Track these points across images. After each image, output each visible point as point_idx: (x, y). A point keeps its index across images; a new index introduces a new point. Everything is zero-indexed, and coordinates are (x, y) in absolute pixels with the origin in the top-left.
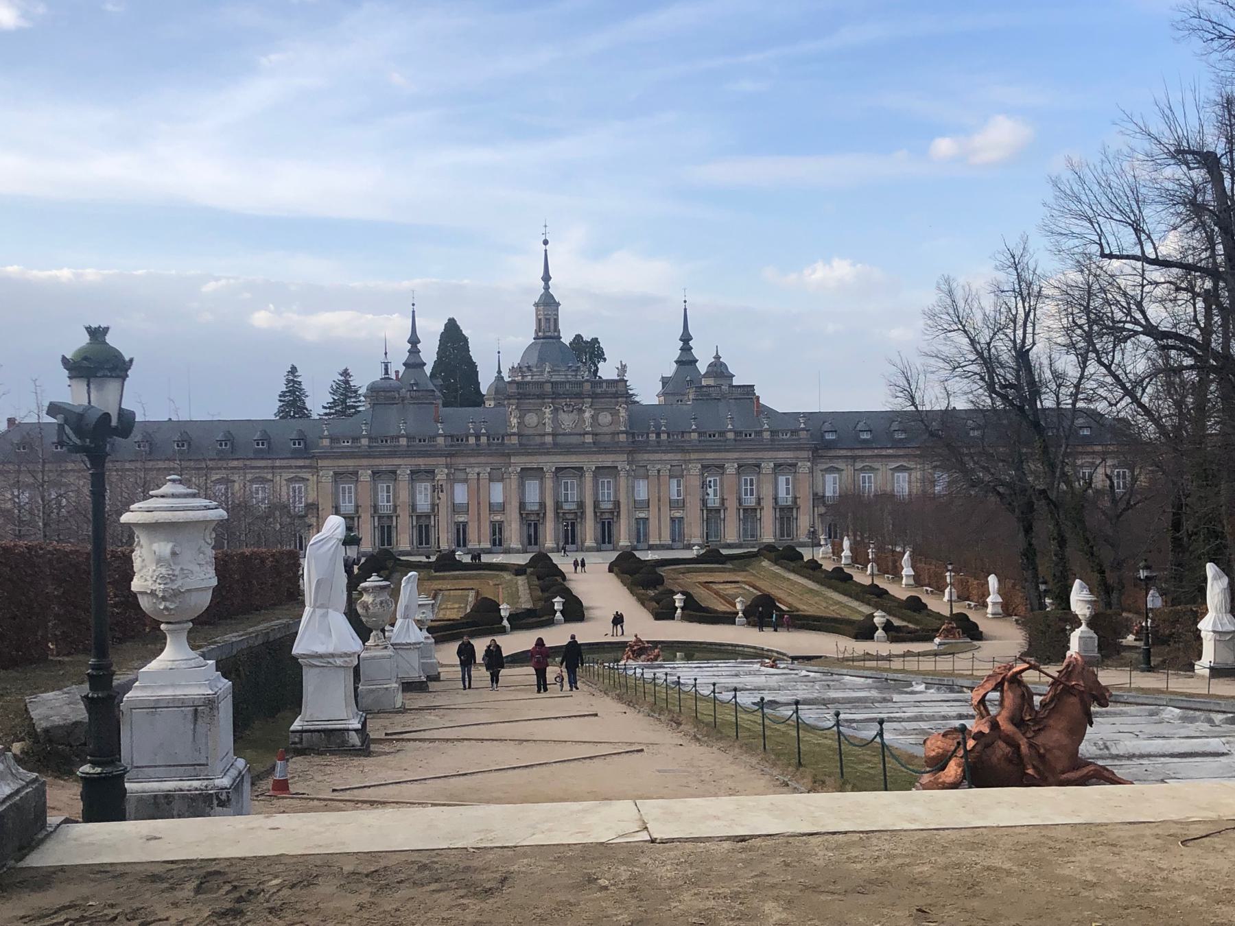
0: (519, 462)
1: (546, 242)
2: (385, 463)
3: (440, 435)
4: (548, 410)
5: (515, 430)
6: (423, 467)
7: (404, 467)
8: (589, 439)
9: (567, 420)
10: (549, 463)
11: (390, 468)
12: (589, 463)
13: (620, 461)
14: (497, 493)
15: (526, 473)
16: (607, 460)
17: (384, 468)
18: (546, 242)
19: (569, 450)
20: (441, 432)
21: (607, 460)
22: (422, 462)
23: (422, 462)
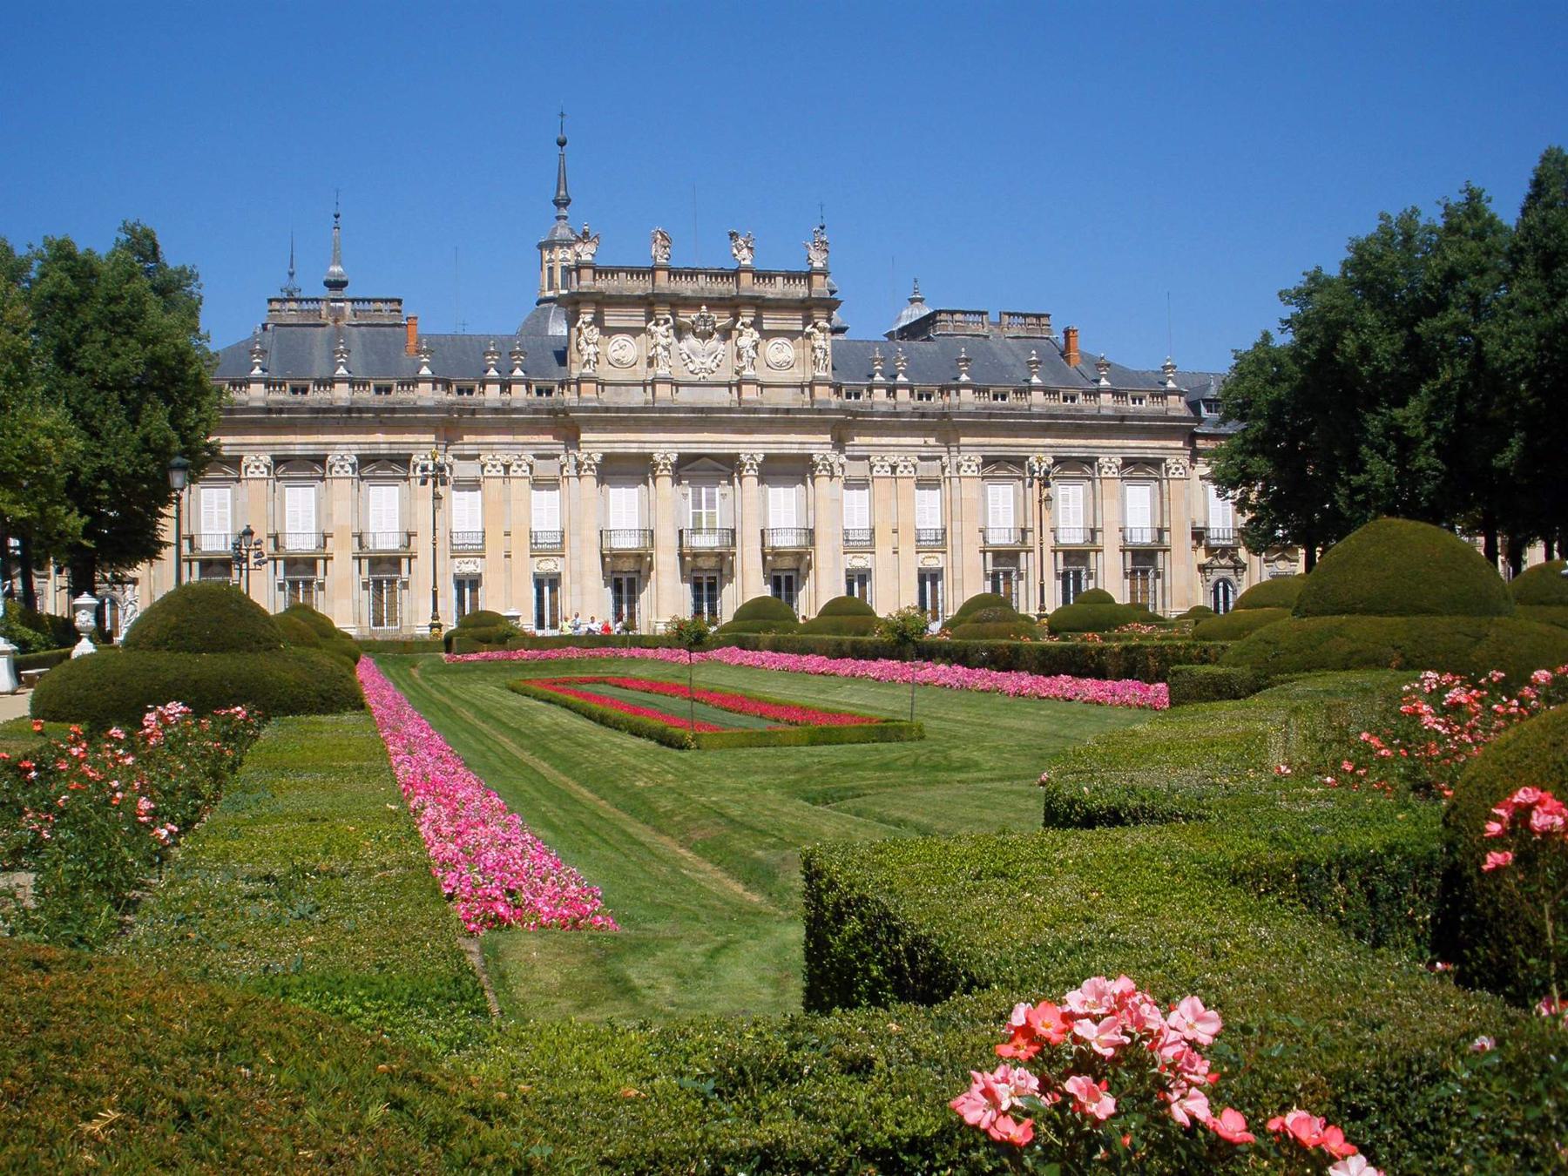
0: (596, 444)
1: (562, 144)
2: (299, 443)
3: (425, 380)
4: (662, 329)
5: (587, 370)
6: (384, 450)
7: (344, 447)
8: (750, 393)
9: (702, 357)
10: (665, 446)
11: (311, 450)
12: (753, 447)
13: (818, 445)
14: (545, 512)
15: (617, 470)
16: (790, 443)
17: (297, 451)
18: (562, 144)
19: (704, 419)
20: (425, 371)
21: (790, 443)
22: (381, 441)
23: (381, 441)
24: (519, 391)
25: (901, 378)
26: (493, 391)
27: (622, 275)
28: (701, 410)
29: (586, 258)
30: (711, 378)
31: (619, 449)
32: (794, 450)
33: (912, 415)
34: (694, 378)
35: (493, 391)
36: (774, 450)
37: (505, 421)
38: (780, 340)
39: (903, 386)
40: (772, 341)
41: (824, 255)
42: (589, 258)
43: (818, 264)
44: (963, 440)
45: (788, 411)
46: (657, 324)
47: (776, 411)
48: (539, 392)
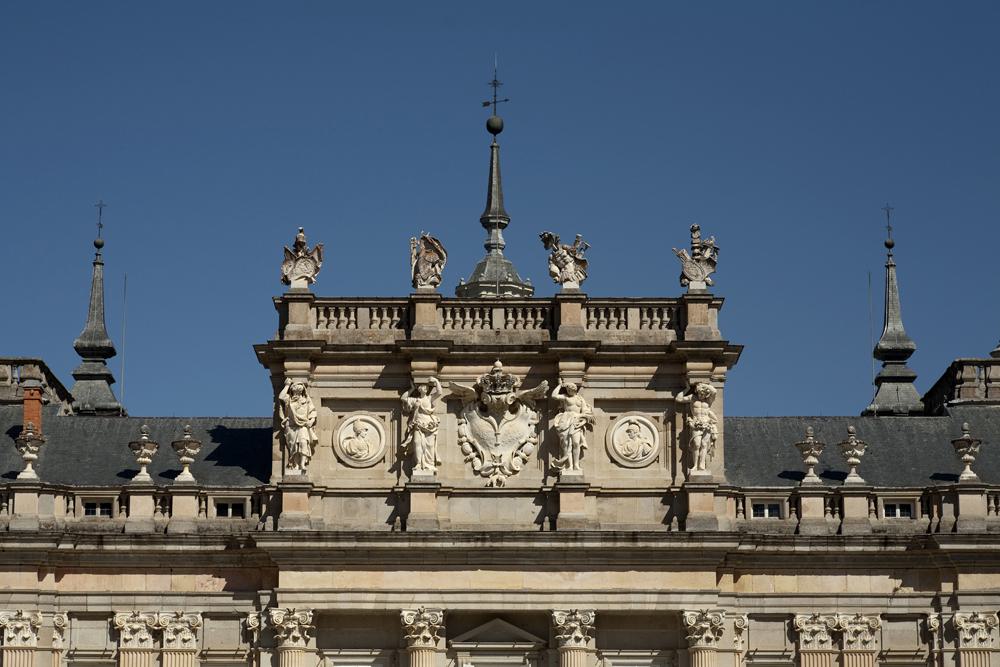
4: (425, 402)
5: (293, 472)
16: (642, 589)
21: (642, 589)
24: (186, 508)
25: (854, 478)
26: (142, 509)
27: (363, 312)
28: (482, 536)
29: (299, 284)
30: (509, 482)
31: (344, 603)
32: (651, 604)
33: (866, 540)
34: (479, 482)
35: (142, 509)
36: (614, 604)
37: (155, 554)
38: (634, 416)
39: (855, 492)
40: (622, 418)
41: (707, 270)
42: (302, 284)
43: (697, 286)
44: (968, 582)
45: (634, 537)
46: (417, 394)
47: (614, 536)
48: (222, 510)
